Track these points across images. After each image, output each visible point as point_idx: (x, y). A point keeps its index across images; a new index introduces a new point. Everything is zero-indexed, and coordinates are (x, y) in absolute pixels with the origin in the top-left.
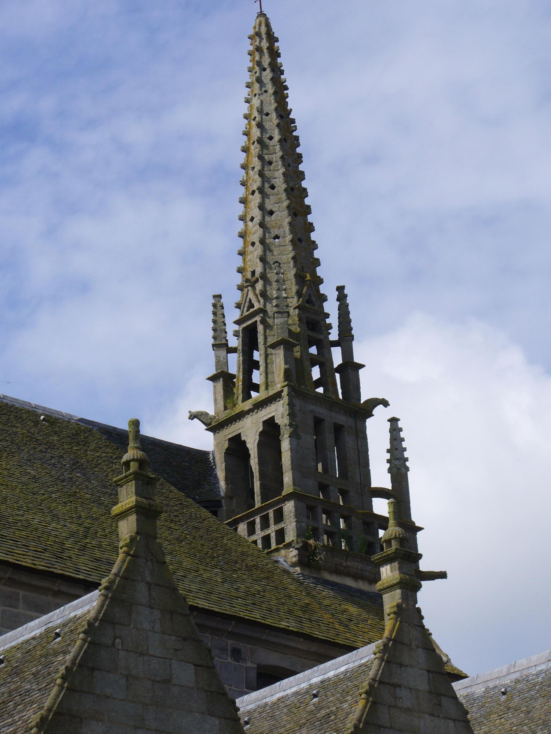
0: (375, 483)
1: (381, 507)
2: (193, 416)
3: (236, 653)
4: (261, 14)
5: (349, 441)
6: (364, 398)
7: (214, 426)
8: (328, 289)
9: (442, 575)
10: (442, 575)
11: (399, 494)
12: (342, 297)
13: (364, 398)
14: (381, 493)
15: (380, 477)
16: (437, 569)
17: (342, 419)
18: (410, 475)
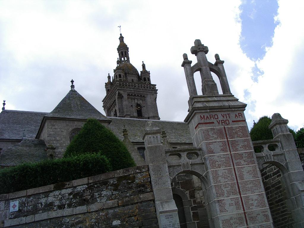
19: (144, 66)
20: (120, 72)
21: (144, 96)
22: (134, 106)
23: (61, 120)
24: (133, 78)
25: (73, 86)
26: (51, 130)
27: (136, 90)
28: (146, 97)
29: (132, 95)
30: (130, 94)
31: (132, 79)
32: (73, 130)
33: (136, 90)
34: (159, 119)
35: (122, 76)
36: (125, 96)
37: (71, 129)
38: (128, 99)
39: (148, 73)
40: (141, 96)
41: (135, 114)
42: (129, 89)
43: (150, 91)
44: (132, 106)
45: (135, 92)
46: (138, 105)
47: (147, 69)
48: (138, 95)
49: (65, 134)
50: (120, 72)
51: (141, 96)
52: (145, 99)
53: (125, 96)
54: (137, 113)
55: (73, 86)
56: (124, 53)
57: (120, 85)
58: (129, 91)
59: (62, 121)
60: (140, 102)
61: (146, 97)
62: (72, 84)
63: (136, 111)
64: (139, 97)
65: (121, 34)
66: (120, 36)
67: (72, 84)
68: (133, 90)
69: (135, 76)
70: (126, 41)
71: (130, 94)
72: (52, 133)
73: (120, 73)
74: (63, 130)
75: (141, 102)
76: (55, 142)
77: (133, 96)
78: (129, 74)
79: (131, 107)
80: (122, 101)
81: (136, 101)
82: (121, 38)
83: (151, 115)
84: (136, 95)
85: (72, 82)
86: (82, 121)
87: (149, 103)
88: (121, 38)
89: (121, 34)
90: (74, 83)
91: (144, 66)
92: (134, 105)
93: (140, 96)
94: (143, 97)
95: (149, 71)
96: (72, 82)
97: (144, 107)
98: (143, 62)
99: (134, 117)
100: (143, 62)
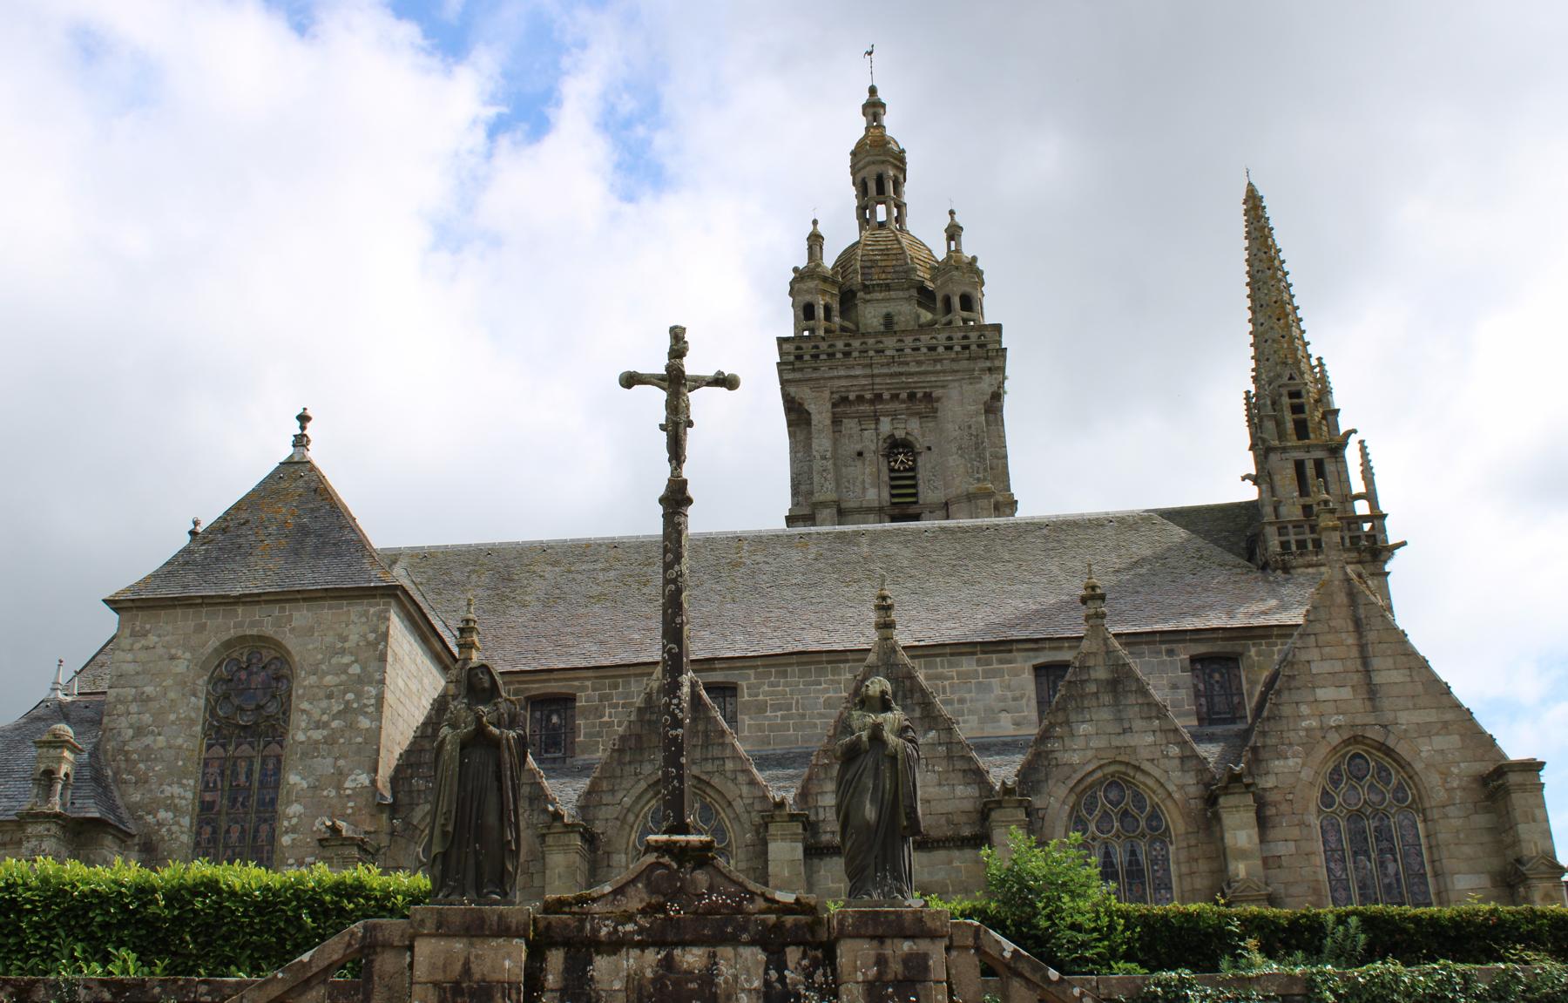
0: (1354, 492)
1: (1362, 508)
2: (1244, 479)
3: (1170, 652)
4: (1250, 184)
5: (1330, 467)
6: (1342, 432)
7: (1256, 480)
8: (1314, 362)
9: (1404, 544)
10: (1404, 544)
11: (1370, 496)
12: (1321, 365)
13: (1342, 432)
14: (1359, 497)
15: (1358, 486)
16: (1399, 541)
17: (1319, 454)
18: (1376, 478)
19: (953, 232)
20: (808, 292)
21: (928, 397)
22: (868, 456)
23: (174, 606)
24: (891, 308)
25: (301, 441)
26: (129, 657)
27: (885, 370)
28: (938, 399)
29: (860, 399)
30: (852, 396)
31: (884, 311)
32: (228, 645)
33: (885, 370)
34: (1012, 505)
35: (820, 313)
36: (820, 413)
37: (214, 643)
38: (836, 421)
39: (972, 269)
40: (912, 396)
41: (876, 495)
42: (842, 373)
43: (964, 364)
44: (860, 454)
45: (878, 380)
46: (897, 446)
47: (968, 252)
48: (895, 397)
49: (180, 667)
50: (808, 292)
51: (912, 396)
52: (936, 411)
53: (820, 413)
54: (893, 487)
55: (301, 441)
56: (872, 186)
57: (799, 358)
58: (843, 383)
59: (179, 611)
60: (913, 428)
61: (938, 399)
62: (303, 428)
63: (886, 479)
64: (903, 402)
65: (873, 90)
66: (865, 97)
67: (303, 428)
68: (868, 371)
69: (906, 294)
70: (892, 124)
71: (852, 396)
72: (129, 668)
73: (808, 298)
74: (180, 653)
75: (914, 426)
76: (134, 708)
77: (872, 402)
78: (866, 289)
79: (859, 463)
80: (809, 438)
81: (886, 426)
82: (874, 108)
83: (962, 484)
84: (886, 396)
85: (303, 419)
86: (267, 602)
87: (950, 426)
88: (874, 108)
89: (873, 90)
90: (309, 425)
91: (953, 232)
92: (873, 447)
93: (904, 395)
94: (925, 403)
95: (974, 259)
96: (303, 419)
97: (929, 449)
98: (952, 213)
99: (864, 512)
100: (952, 213)
